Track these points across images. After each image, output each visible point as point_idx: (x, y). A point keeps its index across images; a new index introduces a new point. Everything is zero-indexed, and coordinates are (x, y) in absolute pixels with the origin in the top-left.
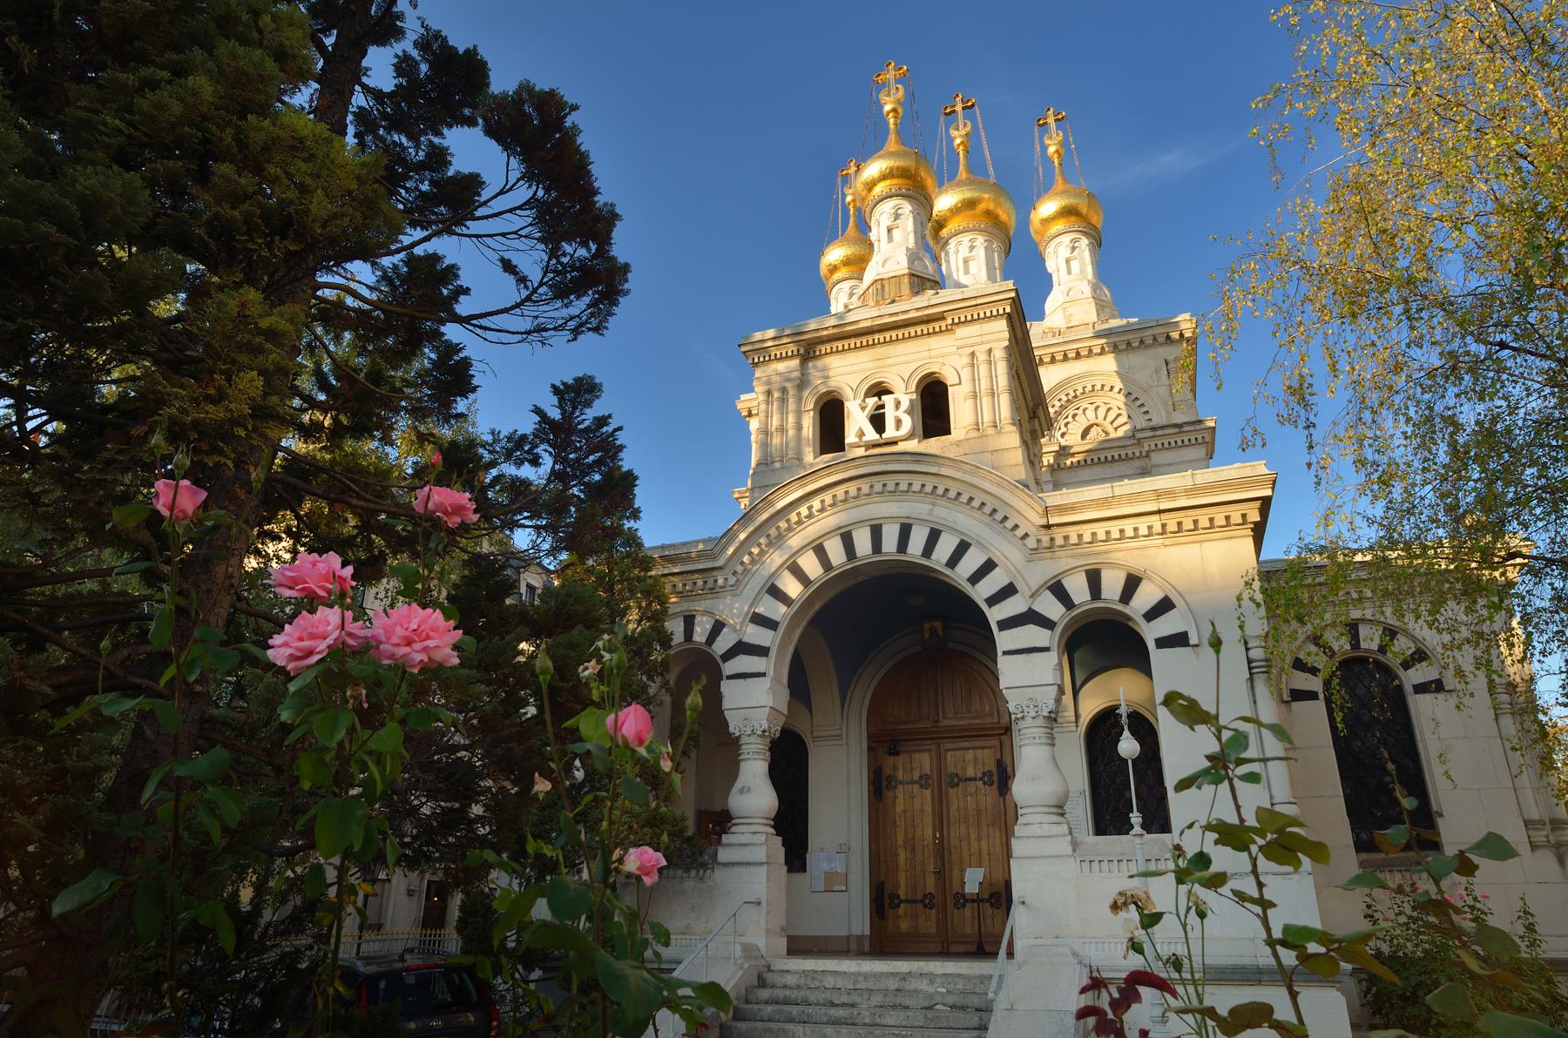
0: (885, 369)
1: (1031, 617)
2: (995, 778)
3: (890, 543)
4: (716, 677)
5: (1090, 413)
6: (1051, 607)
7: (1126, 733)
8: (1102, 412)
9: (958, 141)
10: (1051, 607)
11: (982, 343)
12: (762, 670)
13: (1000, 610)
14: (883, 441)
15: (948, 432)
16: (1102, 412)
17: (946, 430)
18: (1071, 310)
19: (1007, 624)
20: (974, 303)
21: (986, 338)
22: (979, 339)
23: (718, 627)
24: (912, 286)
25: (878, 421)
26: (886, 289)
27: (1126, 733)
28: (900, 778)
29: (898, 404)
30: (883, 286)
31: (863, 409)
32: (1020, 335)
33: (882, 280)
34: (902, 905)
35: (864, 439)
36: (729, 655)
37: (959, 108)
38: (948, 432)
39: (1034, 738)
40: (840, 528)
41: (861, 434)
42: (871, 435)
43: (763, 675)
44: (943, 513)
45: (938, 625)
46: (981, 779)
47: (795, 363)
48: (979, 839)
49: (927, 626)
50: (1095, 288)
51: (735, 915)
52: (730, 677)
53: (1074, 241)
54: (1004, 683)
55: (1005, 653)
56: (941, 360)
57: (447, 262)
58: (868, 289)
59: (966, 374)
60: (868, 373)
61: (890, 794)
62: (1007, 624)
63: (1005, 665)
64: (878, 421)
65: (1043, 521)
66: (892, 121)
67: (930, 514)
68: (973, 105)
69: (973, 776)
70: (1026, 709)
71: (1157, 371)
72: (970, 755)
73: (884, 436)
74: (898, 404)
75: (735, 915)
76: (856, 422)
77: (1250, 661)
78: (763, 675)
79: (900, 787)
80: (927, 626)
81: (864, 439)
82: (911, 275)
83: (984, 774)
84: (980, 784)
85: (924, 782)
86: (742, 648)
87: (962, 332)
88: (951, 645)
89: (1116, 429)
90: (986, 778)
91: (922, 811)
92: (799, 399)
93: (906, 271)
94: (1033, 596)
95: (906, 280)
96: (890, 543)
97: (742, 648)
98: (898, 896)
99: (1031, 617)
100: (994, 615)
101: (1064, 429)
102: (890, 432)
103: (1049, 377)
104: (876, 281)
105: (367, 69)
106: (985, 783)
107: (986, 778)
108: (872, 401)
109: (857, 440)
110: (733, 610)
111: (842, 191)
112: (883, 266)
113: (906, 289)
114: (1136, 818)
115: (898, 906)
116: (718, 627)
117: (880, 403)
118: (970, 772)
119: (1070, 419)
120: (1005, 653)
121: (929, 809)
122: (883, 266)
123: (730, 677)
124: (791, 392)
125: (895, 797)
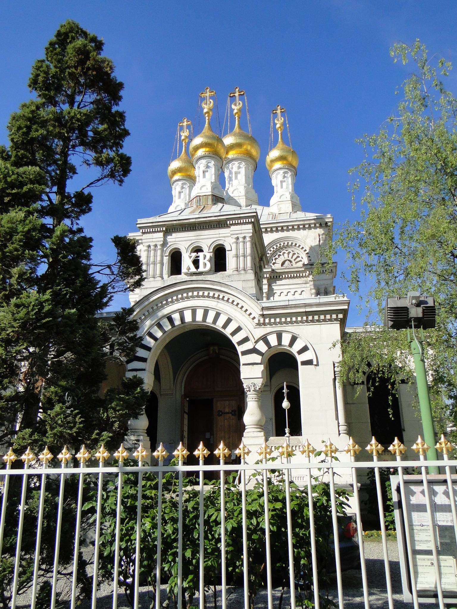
0: (200, 241)
1: (254, 351)
2: (237, 413)
3: (199, 317)
5: (286, 255)
6: (262, 347)
7: (285, 399)
8: (291, 255)
9: (235, 111)
10: (262, 347)
11: (241, 233)
12: (144, 368)
13: (242, 347)
14: (198, 272)
15: (225, 270)
16: (291, 255)
17: (224, 269)
18: (281, 206)
19: (246, 353)
20: (239, 216)
21: (243, 232)
22: (240, 232)
24: (212, 200)
25: (196, 263)
26: (201, 200)
27: (285, 399)
29: (205, 257)
30: (200, 199)
31: (190, 257)
33: (200, 196)
35: (190, 271)
37: (237, 94)
38: (225, 270)
39: (253, 398)
40: (179, 309)
41: (189, 269)
42: (193, 269)
44: (221, 306)
45: (216, 348)
46: (231, 413)
47: (161, 234)
48: (229, 438)
49: (212, 348)
50: (292, 197)
53: (285, 173)
54: (242, 376)
55: (243, 365)
56: (223, 239)
58: (193, 199)
59: (234, 246)
60: (193, 241)
62: (246, 353)
63: (243, 369)
64: (196, 263)
65: (261, 313)
66: (207, 118)
67: (216, 306)
68: (243, 94)
69: (228, 411)
70: (250, 387)
71: (315, 239)
72: (227, 403)
73: (198, 270)
74: (205, 257)
76: (187, 263)
77: (335, 372)
80: (212, 348)
81: (190, 271)
82: (213, 195)
83: (232, 411)
84: (230, 415)
87: (233, 228)
88: (221, 357)
89: (296, 263)
90: (233, 413)
92: (162, 251)
93: (210, 193)
95: (210, 197)
96: (199, 317)
99: (254, 351)
100: (240, 349)
101: (274, 261)
102: (201, 269)
103: (268, 238)
104: (197, 196)
106: (232, 415)
107: (233, 413)
108: (194, 255)
109: (187, 271)
111: (180, 133)
112: (201, 189)
113: (210, 202)
114: (287, 430)
117: (198, 255)
118: (227, 410)
120: (243, 365)
122: (201, 189)
124: (159, 247)
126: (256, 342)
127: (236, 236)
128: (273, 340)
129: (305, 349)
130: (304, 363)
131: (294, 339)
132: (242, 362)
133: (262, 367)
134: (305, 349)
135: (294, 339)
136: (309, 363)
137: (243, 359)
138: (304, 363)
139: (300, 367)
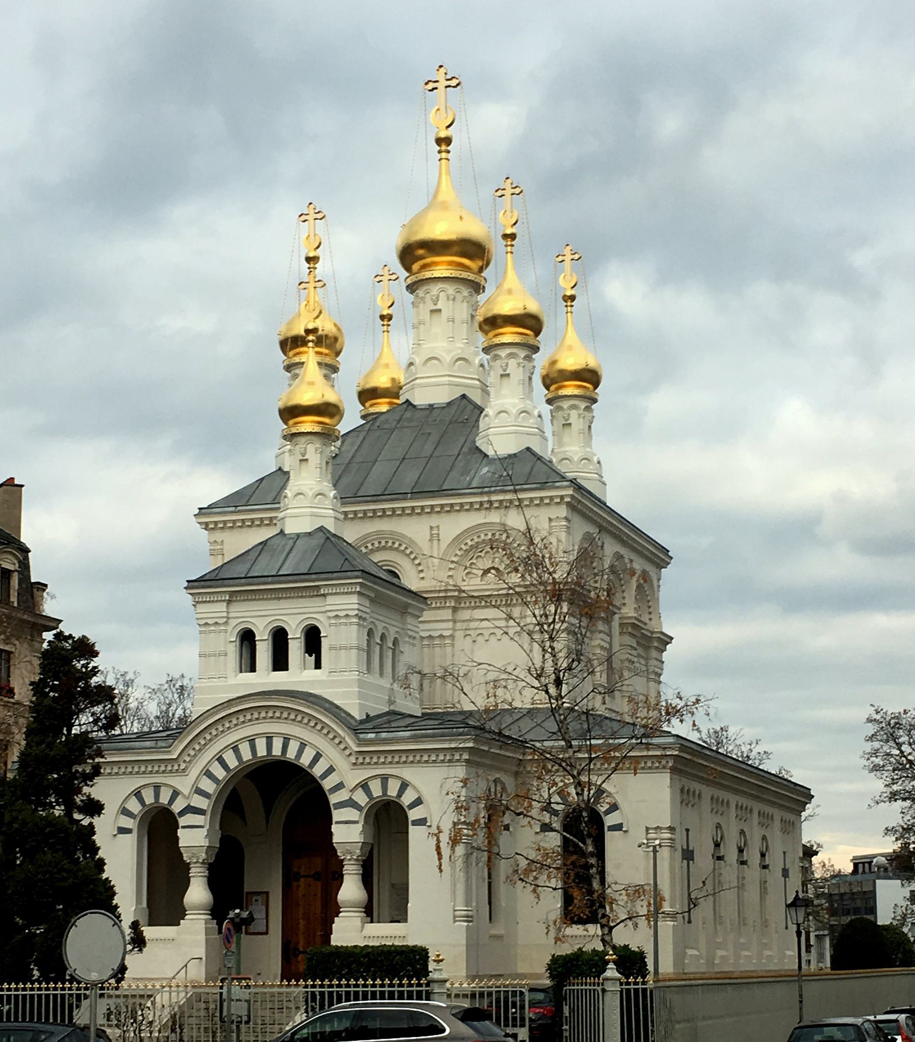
4: (176, 826)
6: (361, 798)
12: (202, 824)
23: (176, 794)
28: (302, 874)
32: (311, 699)
34: (301, 955)
36: (182, 813)
43: (202, 827)
47: (223, 607)
51: (186, 966)
52: (183, 827)
55: (337, 823)
57: (112, 884)
61: (295, 884)
63: (334, 828)
75: (186, 966)
78: (202, 827)
79: (302, 879)
85: (317, 876)
86: (190, 809)
87: (330, 600)
91: (315, 895)
94: (351, 791)
97: (190, 809)
98: (298, 949)
99: (351, 803)
100: (333, 799)
105: (117, 904)
110: (184, 784)
115: (298, 955)
116: (176, 794)
119: (482, 554)
121: (319, 894)
123: (183, 827)
125: (298, 886)
126: (353, 790)
127: (334, 614)
128: (376, 789)
129: (418, 802)
130: (417, 823)
131: (404, 786)
132: (335, 819)
133: (359, 827)
134: (418, 802)
135: (404, 786)
136: (422, 822)
137: (337, 815)
138: (417, 823)
139: (411, 828)
